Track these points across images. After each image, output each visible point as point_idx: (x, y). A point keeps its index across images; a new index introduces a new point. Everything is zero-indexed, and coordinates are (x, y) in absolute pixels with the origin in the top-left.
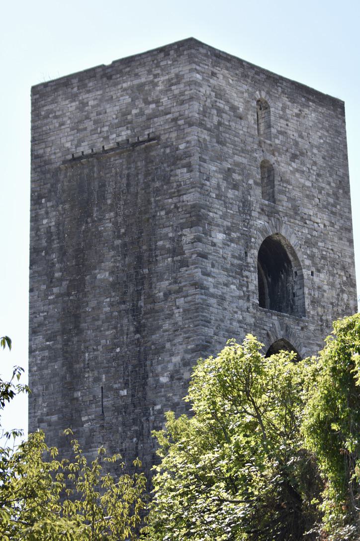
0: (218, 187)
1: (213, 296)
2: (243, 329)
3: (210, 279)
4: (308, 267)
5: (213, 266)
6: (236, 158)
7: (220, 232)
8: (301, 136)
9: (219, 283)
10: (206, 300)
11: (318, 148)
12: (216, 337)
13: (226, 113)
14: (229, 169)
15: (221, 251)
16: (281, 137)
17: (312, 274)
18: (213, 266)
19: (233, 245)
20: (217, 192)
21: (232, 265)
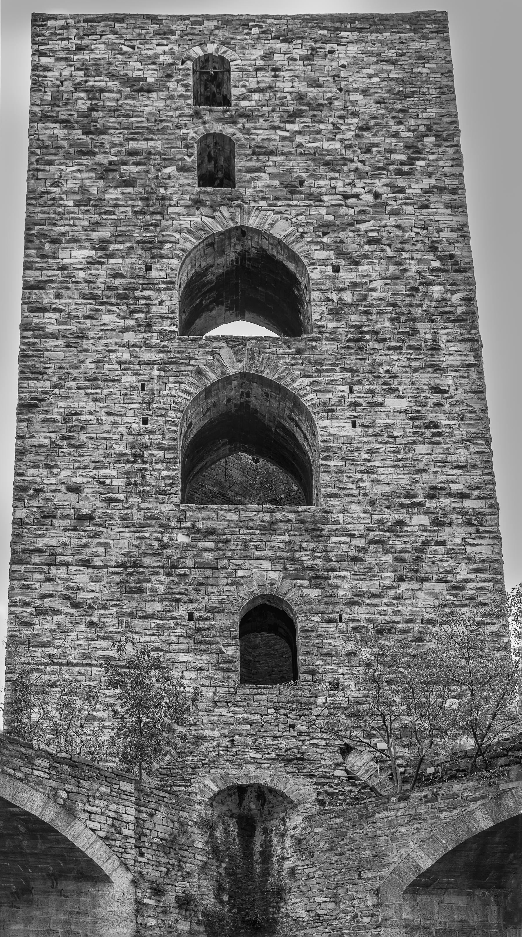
0: (83, 190)
1: (54, 336)
2: (129, 372)
3: (47, 315)
4: (324, 262)
5: (58, 296)
6: (132, 145)
7: (81, 248)
8: (315, 84)
9: (70, 317)
10: (34, 344)
11: (365, 92)
12: (56, 391)
13: (111, 91)
14: (110, 163)
15: (81, 274)
16: (255, 96)
17: (336, 269)
18: (58, 296)
19: (112, 261)
20: (78, 197)
21: (109, 288)
